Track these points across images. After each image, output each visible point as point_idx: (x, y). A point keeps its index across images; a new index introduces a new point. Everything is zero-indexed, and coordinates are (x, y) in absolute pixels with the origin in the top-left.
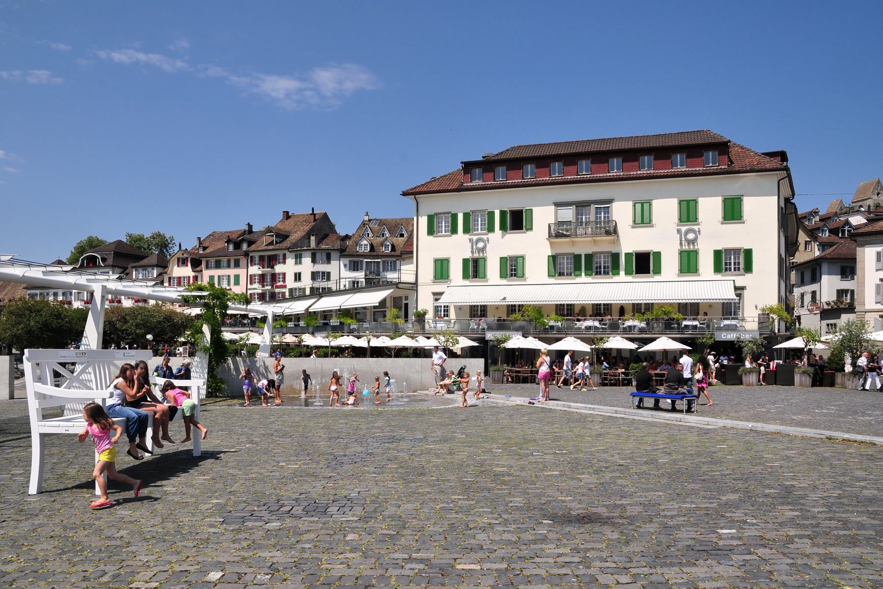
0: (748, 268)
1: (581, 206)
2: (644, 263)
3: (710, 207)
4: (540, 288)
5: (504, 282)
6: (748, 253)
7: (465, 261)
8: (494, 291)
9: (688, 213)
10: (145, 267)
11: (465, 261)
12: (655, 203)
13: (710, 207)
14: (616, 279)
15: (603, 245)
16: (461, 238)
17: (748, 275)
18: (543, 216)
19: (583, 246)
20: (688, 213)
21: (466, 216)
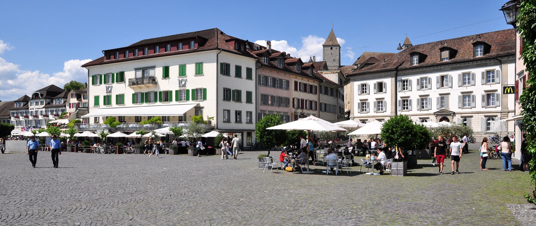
0: (205, 98)
1: (144, 70)
2: (166, 97)
3: (191, 69)
4: (130, 109)
5: (134, 105)
6: (205, 90)
7: (104, 97)
8: (115, 111)
9: (182, 72)
10: (59, 98)
11: (104, 97)
12: (187, 66)
13: (191, 69)
14: (171, 103)
15: (151, 88)
16: (104, 86)
17: (205, 101)
18: (130, 75)
19: (144, 89)
20: (182, 72)
21: (105, 75)
